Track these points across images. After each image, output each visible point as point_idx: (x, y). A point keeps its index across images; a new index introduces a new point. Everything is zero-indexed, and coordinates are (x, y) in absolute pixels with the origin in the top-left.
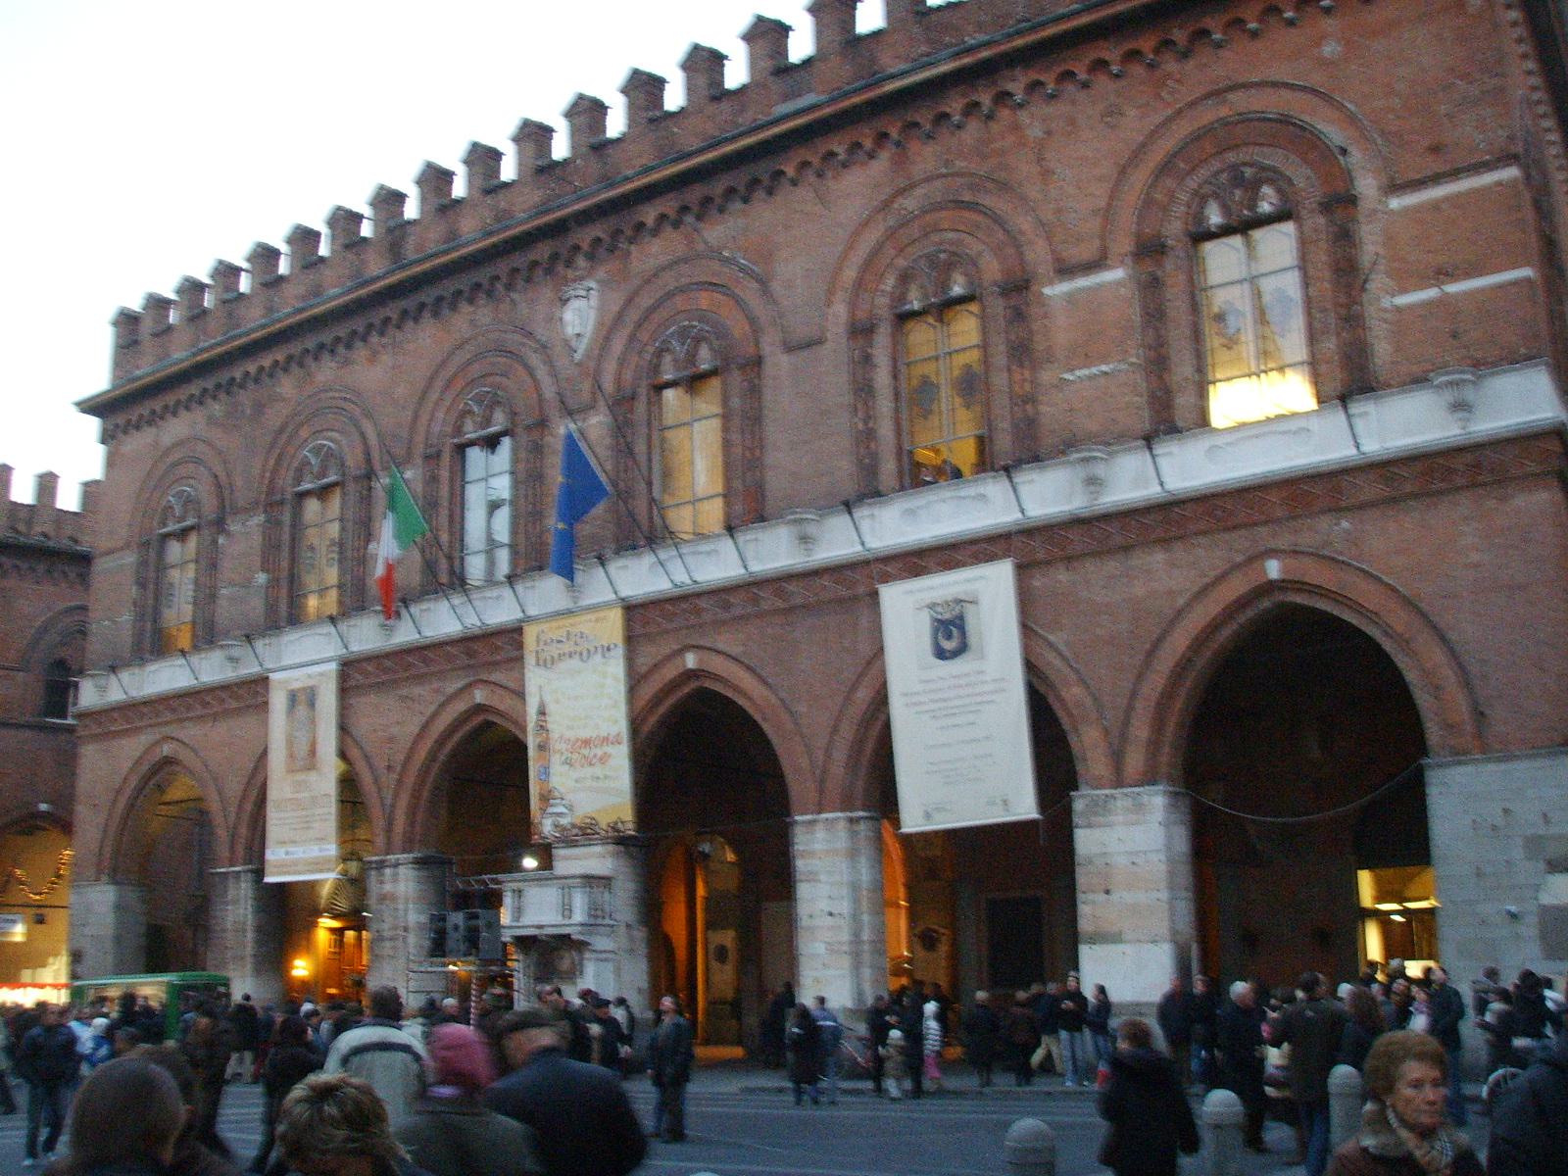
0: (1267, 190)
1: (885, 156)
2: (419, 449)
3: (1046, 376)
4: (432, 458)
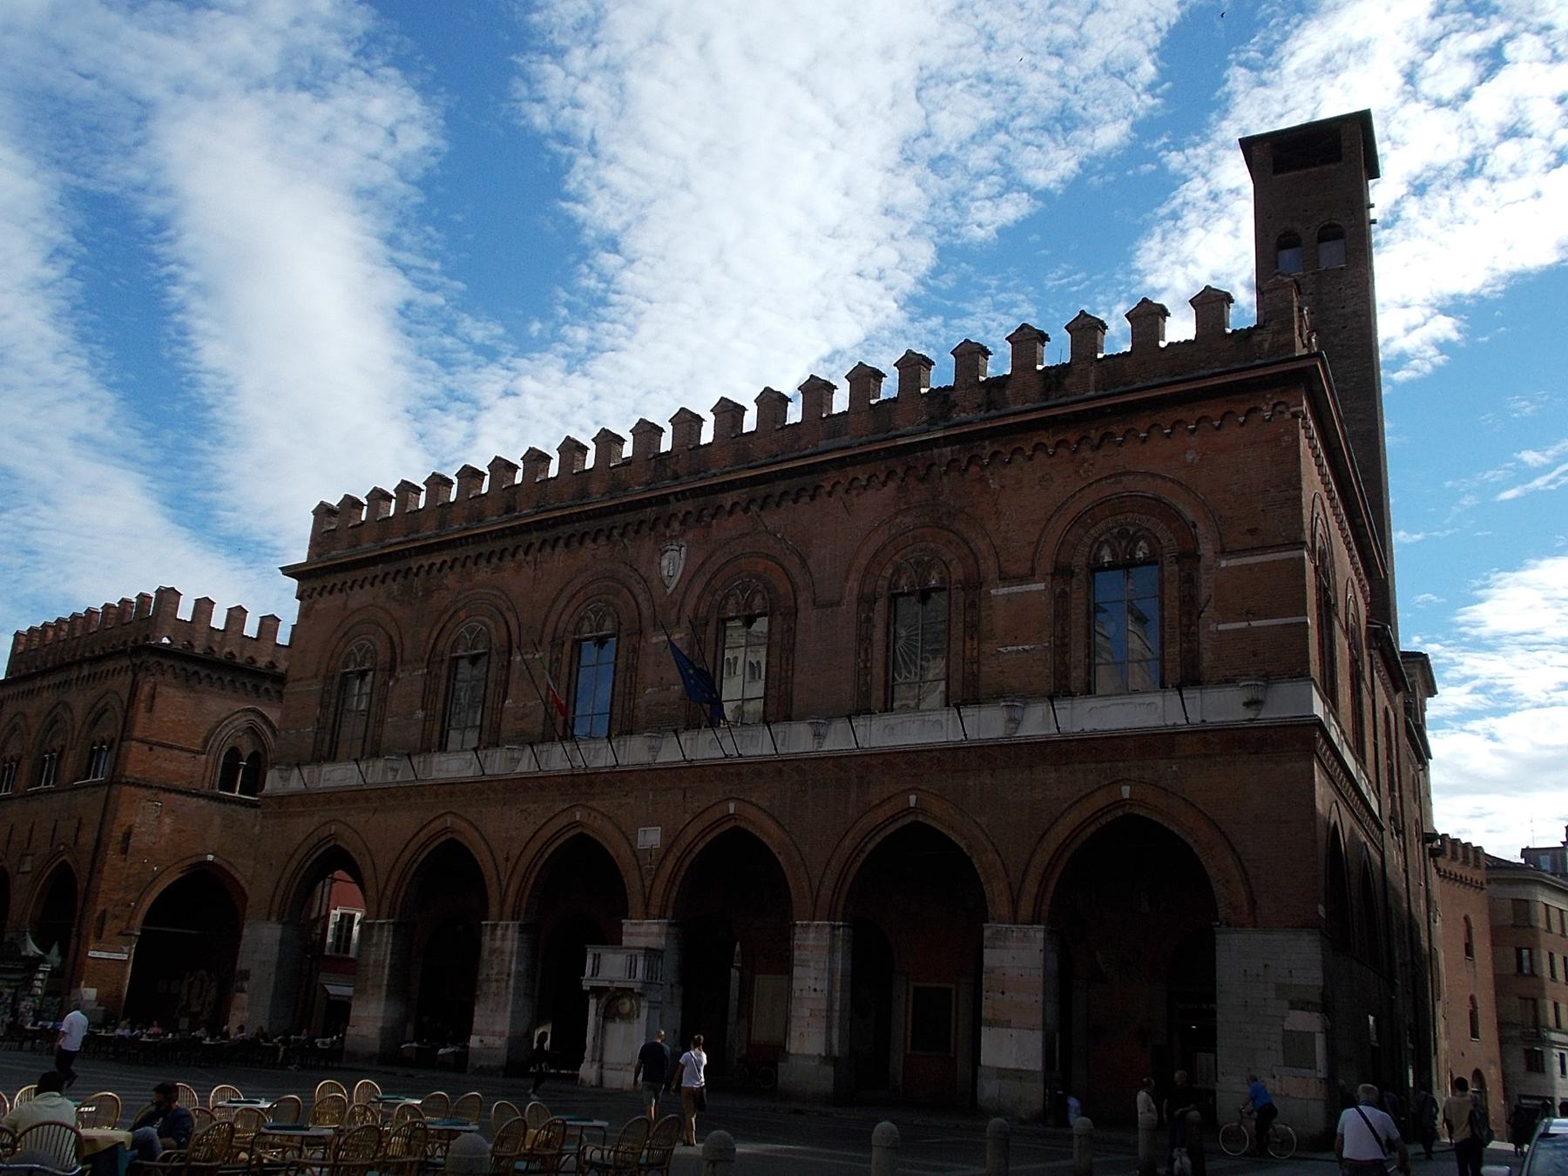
0: (1141, 543)
1: (892, 485)
2: (547, 639)
3: (986, 648)
4: (557, 643)
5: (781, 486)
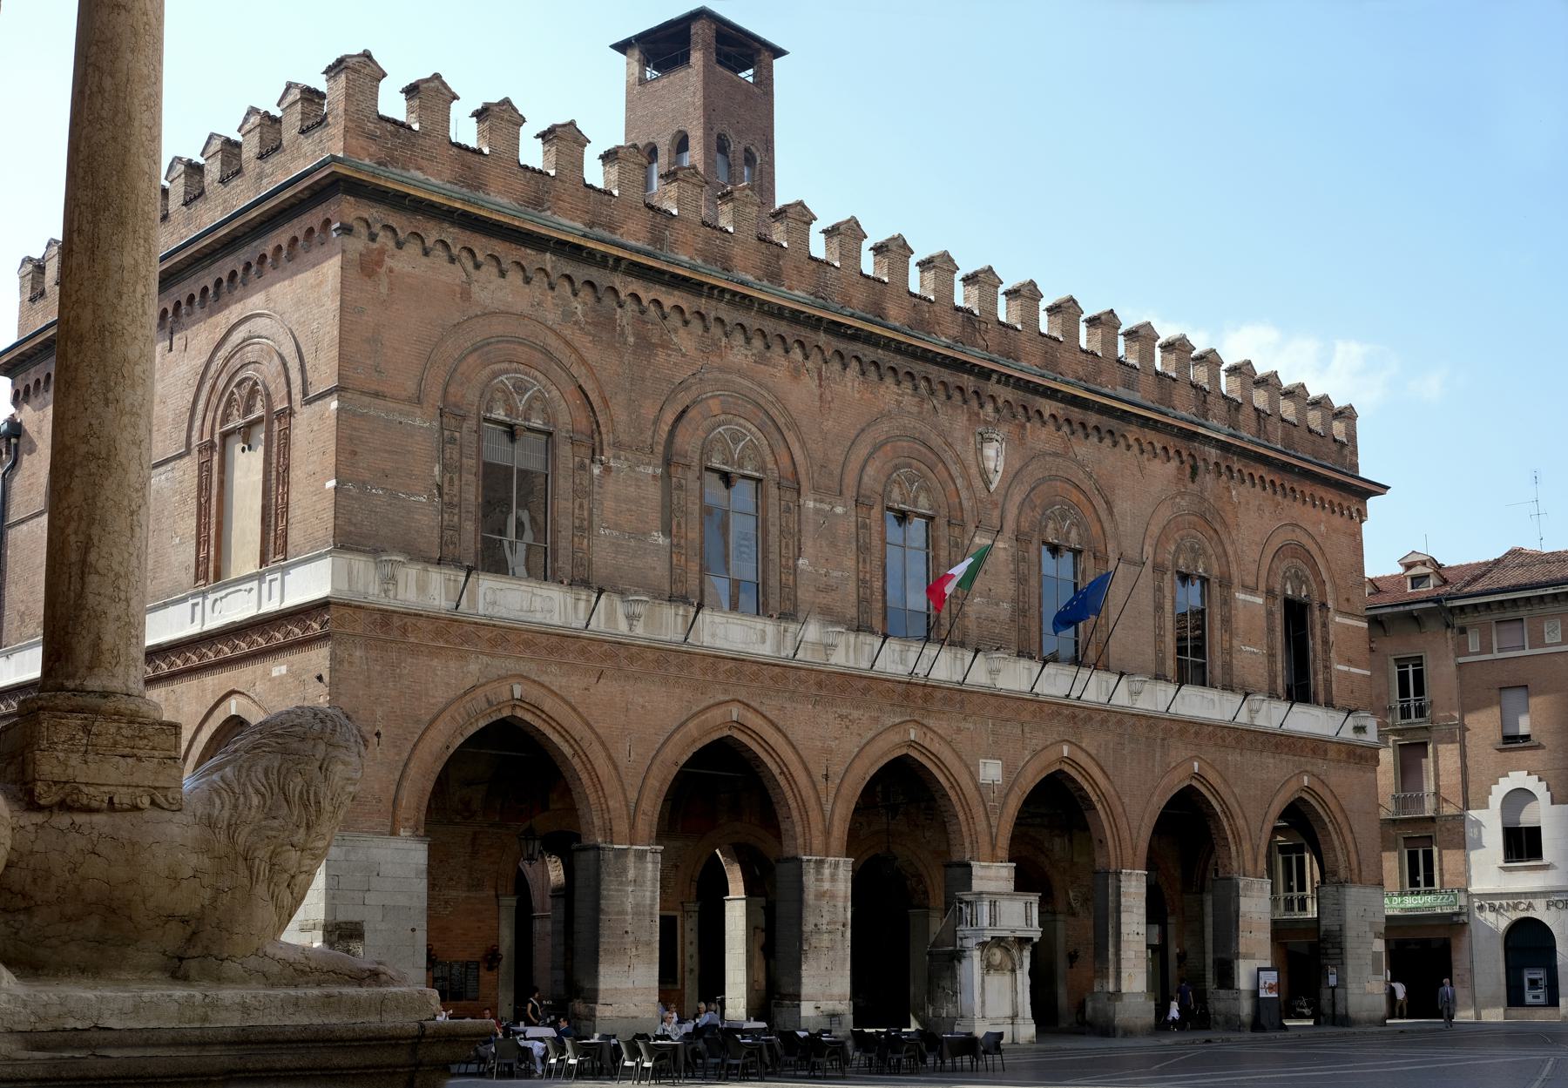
2: (850, 492)
5: (1093, 419)
